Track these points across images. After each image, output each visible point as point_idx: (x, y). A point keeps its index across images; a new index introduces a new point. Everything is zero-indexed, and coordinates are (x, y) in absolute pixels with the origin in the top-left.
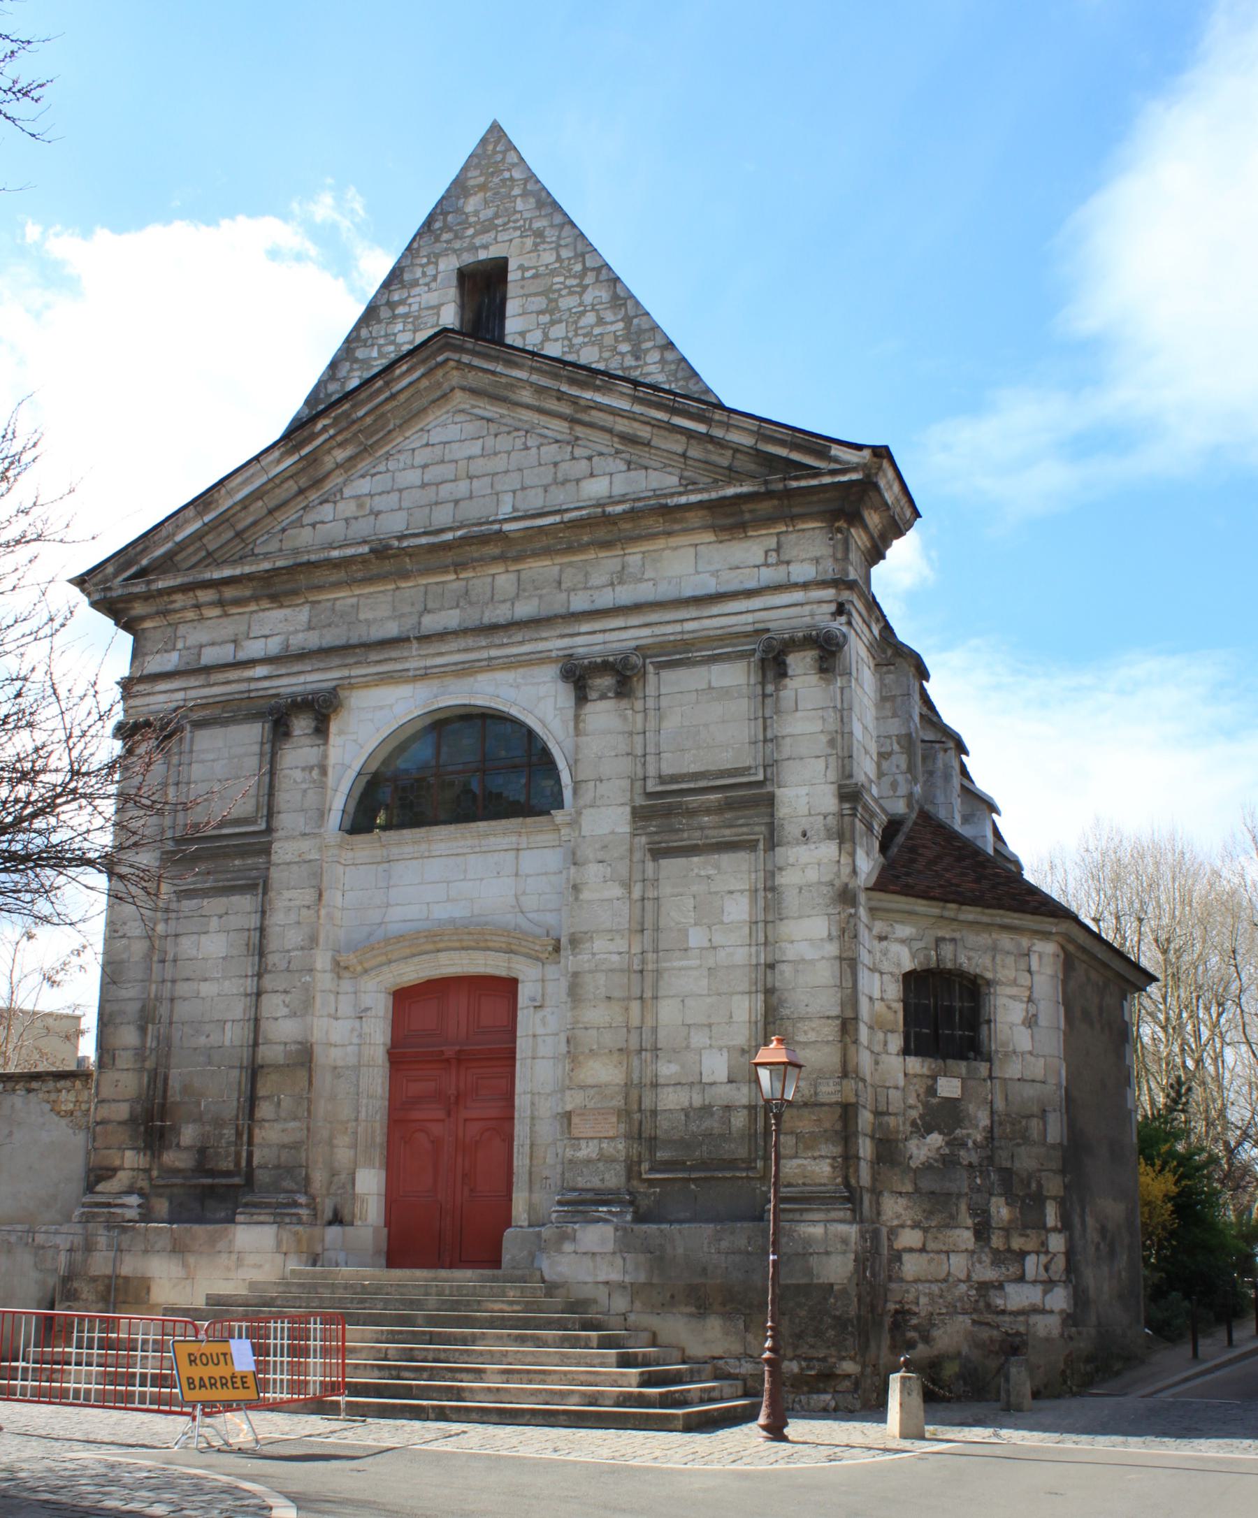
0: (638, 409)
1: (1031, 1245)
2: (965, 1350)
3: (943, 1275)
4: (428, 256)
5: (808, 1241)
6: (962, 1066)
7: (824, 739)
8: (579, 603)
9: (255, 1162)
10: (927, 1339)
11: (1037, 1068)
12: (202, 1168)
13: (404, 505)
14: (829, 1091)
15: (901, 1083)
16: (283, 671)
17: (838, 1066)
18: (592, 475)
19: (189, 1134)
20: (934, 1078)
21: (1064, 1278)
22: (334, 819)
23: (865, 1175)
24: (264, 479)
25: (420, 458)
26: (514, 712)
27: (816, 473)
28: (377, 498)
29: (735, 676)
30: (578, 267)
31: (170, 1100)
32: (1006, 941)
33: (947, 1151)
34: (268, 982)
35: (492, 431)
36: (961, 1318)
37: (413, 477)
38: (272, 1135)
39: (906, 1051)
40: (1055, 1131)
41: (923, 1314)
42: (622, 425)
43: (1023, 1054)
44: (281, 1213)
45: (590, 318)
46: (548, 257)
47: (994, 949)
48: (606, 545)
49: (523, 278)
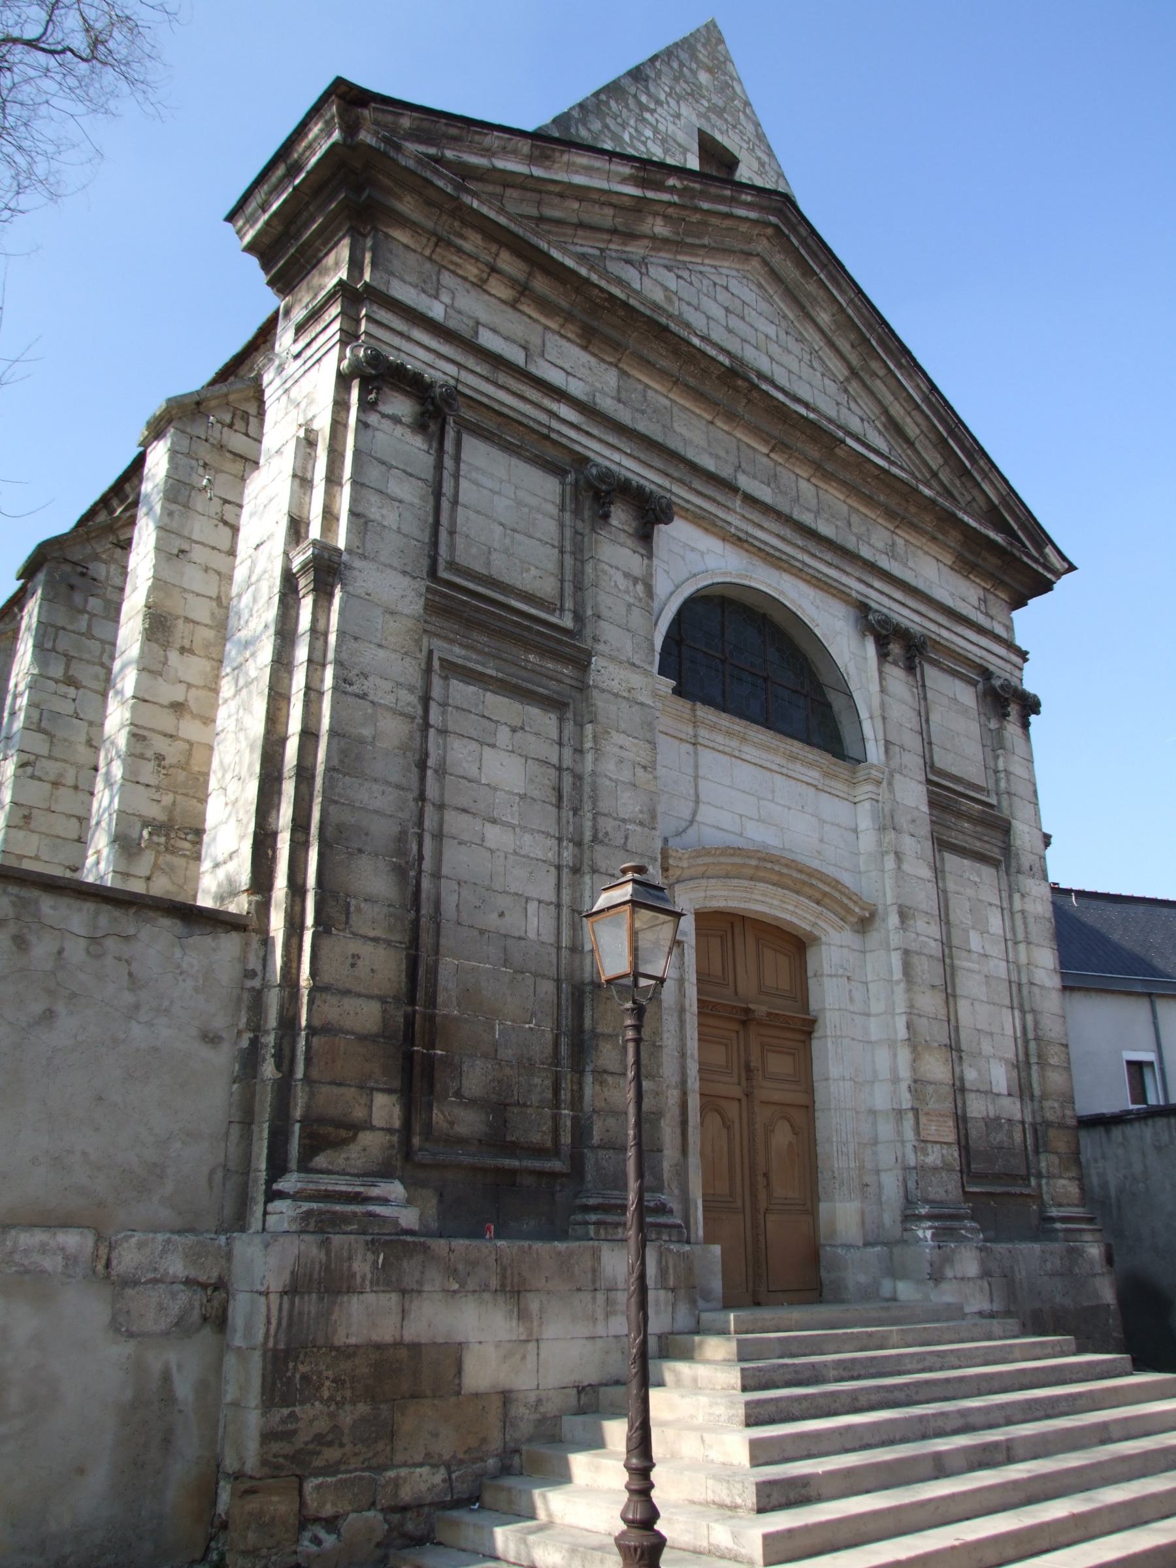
12: (498, 1139)
19: (475, 1078)
31: (441, 1011)
42: (897, 410)
48: (890, 514)
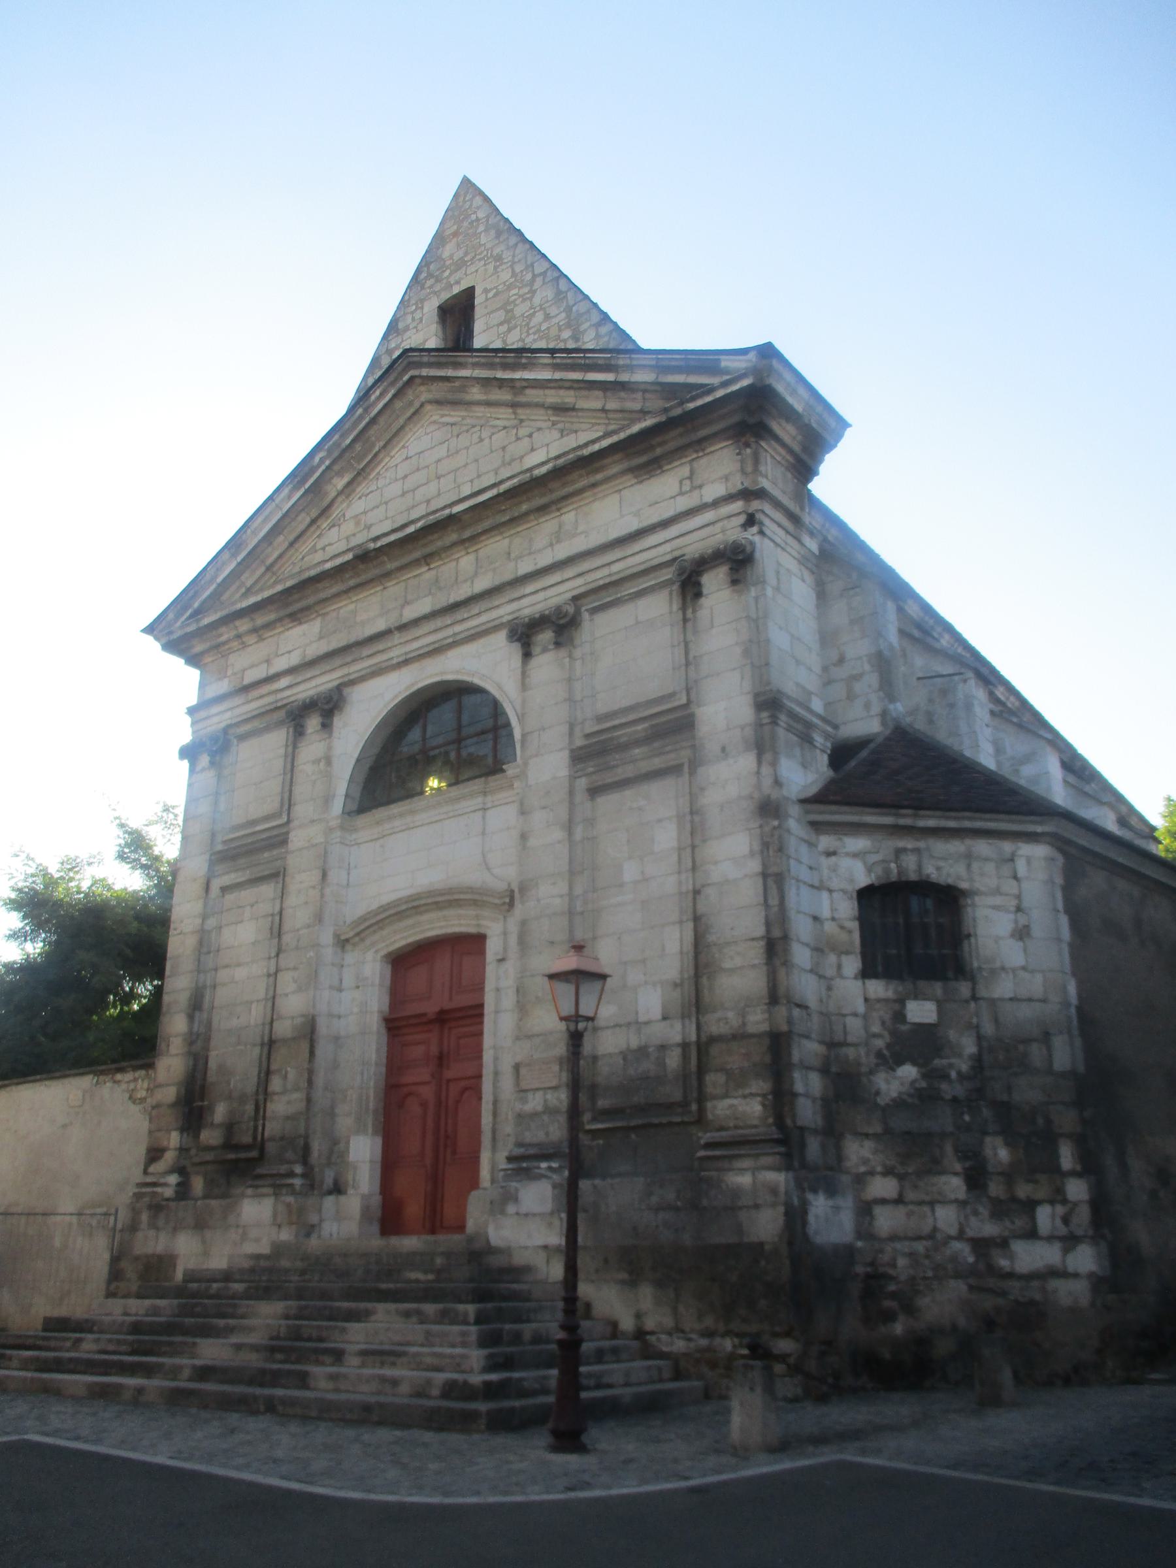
0: (558, 375)
1: (1040, 1194)
2: (962, 1322)
3: (927, 1230)
4: (416, 304)
5: (736, 1192)
6: (938, 988)
7: (738, 650)
8: (525, 567)
9: (266, 1134)
10: (910, 1309)
11: (1035, 985)
13: (390, 514)
14: (757, 1021)
15: (861, 1009)
16: (299, 679)
17: (765, 992)
18: (533, 450)
19: (220, 1112)
20: (901, 1002)
21: (1090, 1232)
22: (338, 806)
23: (807, 1113)
24: (280, 515)
25: (400, 474)
26: (477, 681)
27: (711, 389)
28: (370, 514)
29: (658, 607)
30: (529, 276)
32: (982, 847)
33: (924, 1084)
34: (284, 961)
35: (455, 433)
36: (952, 1283)
37: (396, 489)
38: (282, 1106)
39: (867, 973)
40: (1064, 1054)
41: (903, 1278)
42: (552, 397)
43: (1014, 970)
44: (278, 1185)
45: (540, 316)
46: (505, 275)
47: (969, 857)
48: (542, 509)
49: (487, 300)
